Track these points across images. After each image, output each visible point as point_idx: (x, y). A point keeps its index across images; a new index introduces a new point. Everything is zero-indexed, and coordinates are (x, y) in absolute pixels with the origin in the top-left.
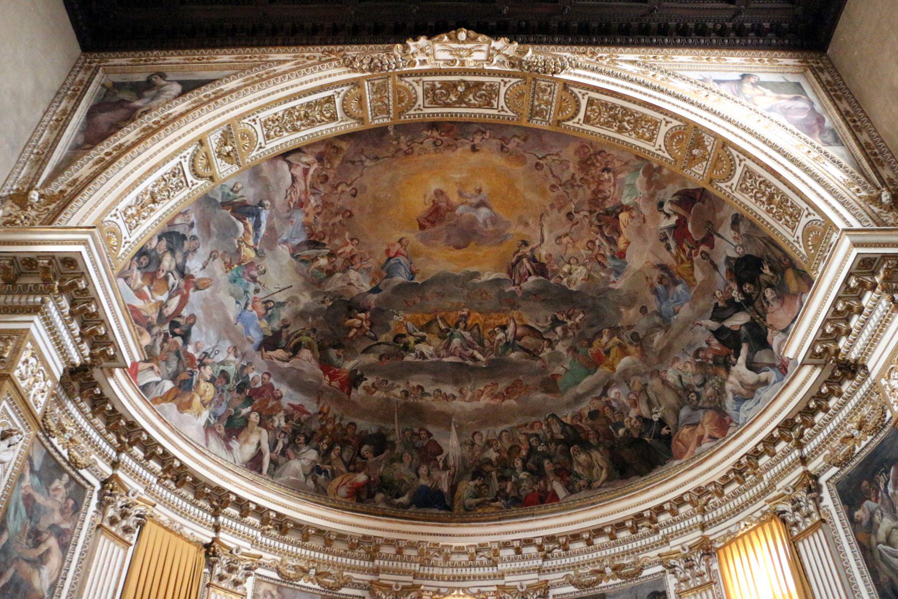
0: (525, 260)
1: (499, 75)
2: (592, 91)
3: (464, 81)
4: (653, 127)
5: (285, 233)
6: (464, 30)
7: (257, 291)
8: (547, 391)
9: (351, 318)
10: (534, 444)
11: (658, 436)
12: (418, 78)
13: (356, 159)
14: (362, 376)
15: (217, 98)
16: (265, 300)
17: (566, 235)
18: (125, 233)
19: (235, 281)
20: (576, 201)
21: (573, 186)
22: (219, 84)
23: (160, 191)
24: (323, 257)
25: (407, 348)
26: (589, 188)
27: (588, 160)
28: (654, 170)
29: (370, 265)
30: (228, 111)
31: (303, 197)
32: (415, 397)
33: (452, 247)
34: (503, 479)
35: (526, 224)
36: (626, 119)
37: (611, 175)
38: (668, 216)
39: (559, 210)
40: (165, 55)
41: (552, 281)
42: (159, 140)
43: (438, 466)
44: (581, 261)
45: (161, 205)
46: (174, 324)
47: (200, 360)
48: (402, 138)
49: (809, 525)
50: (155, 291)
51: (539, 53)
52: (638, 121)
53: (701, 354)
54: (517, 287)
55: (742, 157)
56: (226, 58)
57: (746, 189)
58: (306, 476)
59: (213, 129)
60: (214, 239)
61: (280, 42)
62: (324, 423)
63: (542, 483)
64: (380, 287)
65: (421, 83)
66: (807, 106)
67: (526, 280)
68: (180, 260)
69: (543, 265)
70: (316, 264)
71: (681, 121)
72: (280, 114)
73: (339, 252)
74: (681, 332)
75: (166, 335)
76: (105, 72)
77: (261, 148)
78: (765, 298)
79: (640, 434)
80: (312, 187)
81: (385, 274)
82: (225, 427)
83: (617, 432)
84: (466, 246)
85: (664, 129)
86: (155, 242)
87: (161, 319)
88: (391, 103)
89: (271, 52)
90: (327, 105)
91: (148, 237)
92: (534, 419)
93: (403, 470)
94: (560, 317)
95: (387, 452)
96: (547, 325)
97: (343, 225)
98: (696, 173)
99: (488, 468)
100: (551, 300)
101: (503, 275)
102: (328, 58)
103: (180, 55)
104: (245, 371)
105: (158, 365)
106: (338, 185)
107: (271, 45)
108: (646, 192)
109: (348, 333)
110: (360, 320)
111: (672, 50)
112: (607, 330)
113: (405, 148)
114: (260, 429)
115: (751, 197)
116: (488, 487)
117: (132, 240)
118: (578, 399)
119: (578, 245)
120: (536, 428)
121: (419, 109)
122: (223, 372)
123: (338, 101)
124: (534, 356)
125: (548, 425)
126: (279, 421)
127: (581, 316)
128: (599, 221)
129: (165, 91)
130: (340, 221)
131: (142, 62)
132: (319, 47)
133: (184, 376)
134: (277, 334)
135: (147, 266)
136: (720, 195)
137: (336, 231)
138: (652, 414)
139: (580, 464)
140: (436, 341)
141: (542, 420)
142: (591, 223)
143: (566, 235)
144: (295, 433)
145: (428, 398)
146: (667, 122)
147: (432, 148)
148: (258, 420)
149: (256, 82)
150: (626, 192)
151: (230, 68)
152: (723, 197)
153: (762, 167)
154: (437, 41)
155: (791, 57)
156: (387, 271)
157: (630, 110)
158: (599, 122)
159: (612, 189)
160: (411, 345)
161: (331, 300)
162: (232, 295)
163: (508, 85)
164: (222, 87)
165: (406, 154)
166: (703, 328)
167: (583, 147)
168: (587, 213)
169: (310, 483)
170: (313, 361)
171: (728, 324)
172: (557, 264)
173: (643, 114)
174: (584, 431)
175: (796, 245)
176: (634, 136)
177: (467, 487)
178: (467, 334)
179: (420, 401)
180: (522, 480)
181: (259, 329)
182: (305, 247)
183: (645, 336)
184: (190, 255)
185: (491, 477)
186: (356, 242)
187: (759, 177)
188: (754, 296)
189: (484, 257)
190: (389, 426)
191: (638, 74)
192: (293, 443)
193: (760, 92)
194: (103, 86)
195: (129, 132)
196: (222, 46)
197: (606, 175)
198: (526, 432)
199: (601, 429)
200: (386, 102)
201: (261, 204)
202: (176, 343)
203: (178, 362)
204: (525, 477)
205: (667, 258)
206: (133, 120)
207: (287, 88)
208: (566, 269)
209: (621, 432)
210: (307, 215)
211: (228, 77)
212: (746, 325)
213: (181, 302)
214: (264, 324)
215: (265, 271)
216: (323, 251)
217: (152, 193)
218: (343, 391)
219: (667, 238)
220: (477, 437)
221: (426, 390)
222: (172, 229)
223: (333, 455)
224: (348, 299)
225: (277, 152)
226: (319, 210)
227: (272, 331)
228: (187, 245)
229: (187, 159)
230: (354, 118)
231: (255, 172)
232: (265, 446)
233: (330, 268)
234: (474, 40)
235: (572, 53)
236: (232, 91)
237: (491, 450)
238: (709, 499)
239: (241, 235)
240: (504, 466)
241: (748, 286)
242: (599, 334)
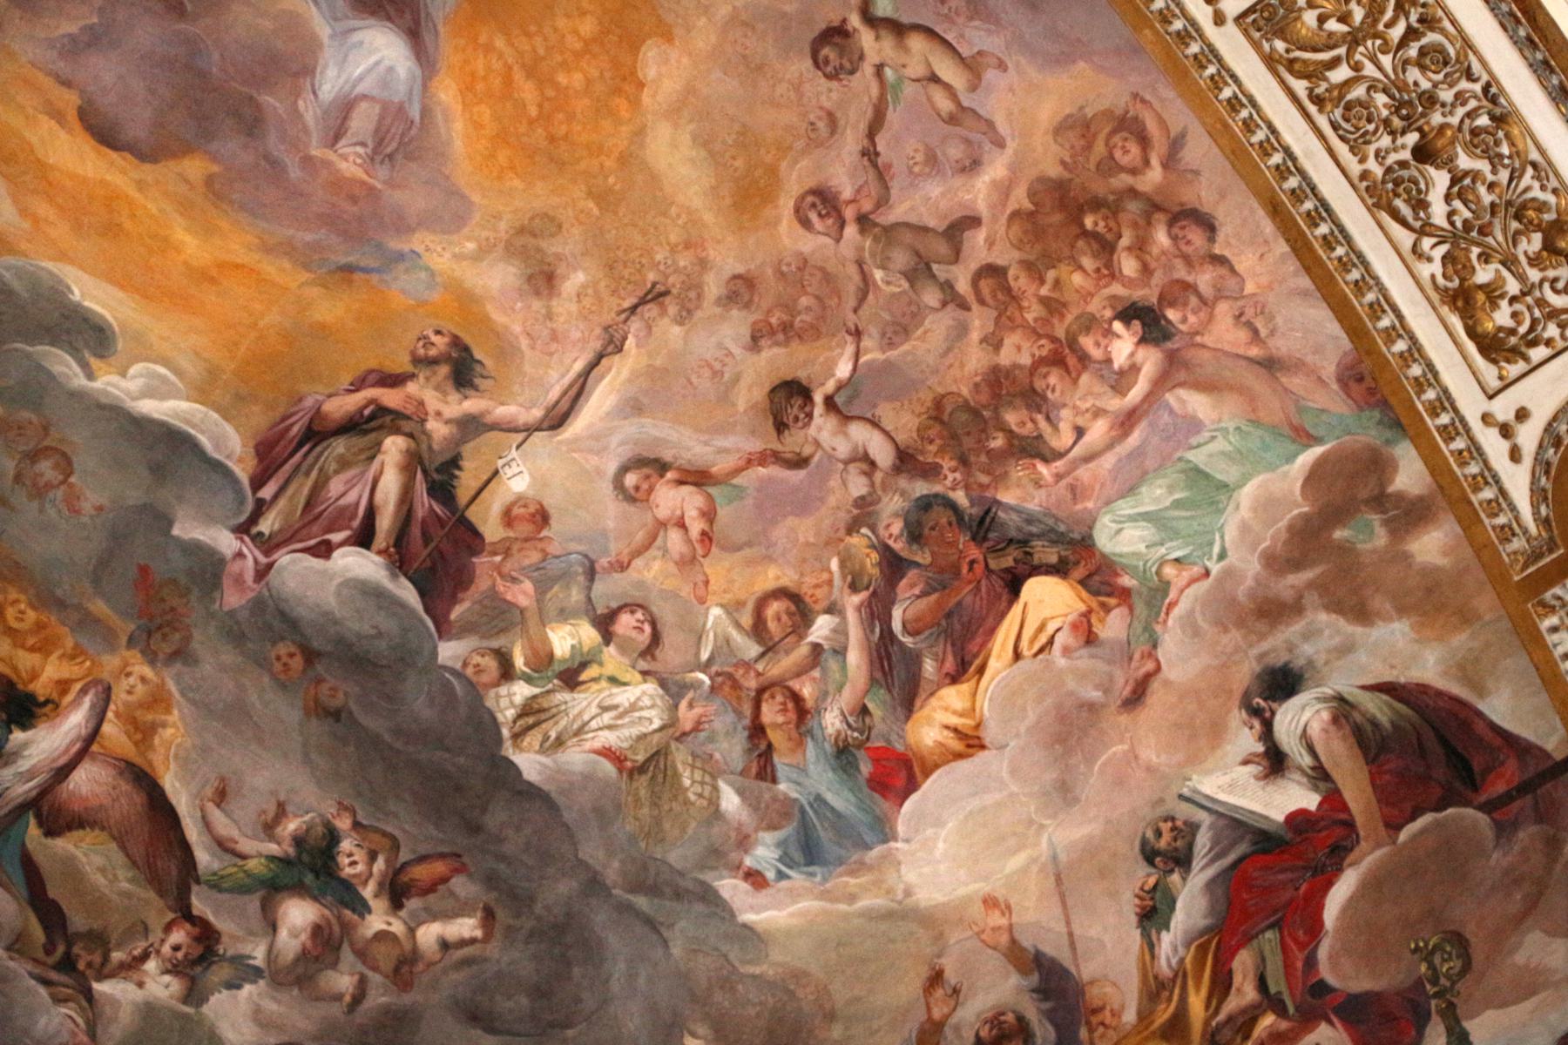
17: (698, 478)
20: (872, 355)
21: (920, 271)
26: (993, 342)
27: (1096, 204)
28: (1380, 501)
33: (70, 100)
35: (543, 280)
36: (1464, 162)
37: (1150, 361)
38: (1274, 762)
41: (449, 652)
44: (671, 655)
54: (252, 555)
67: (324, 550)
69: (468, 537)
84: (145, 154)
94: (351, 857)
96: (259, 850)
100: (376, 741)
108: (1252, 567)
119: (718, 568)
124: (67, 964)
127: (466, 927)
128: (915, 534)
142: (863, 514)
143: (698, 478)
150: (1156, 495)
159: (1098, 431)
168: (883, 453)
172: (542, 588)
189: (204, 277)
197: (1124, 346)
208: (563, 640)
219: (1181, 860)
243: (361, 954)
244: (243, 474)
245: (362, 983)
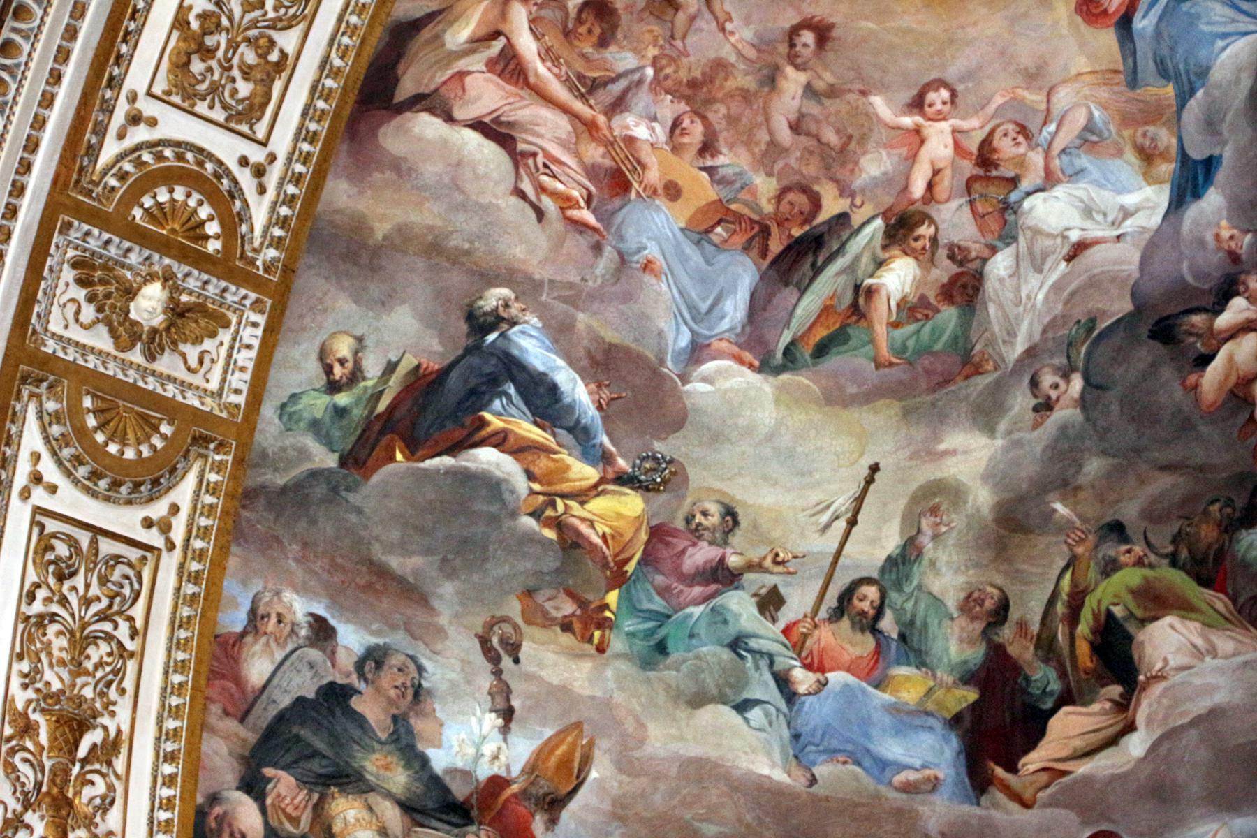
5: (664, 323)
7: (770, 602)
9: (1204, 360)
16: (831, 600)
19: (661, 648)
24: (880, 264)
29: (1079, 119)
31: (594, 153)
60: (446, 592)
64: (1196, 154)
68: (399, 779)
70: (881, 312)
77: (259, 172)
80: (588, 87)
81: (1170, 90)
97: (833, 92)
130: (809, 90)
137: (831, 137)
156: (1164, 72)
162: (698, 700)
170: (1225, 643)
182: (790, 294)
184: (418, 724)
201: (480, 323)
210: (673, 191)
215: (731, 515)
216: (857, 245)
222: (264, 715)
224: (1125, 306)
226: (696, 132)
227: (968, 678)
228: (369, 706)
233: (944, 270)
239: (521, 484)
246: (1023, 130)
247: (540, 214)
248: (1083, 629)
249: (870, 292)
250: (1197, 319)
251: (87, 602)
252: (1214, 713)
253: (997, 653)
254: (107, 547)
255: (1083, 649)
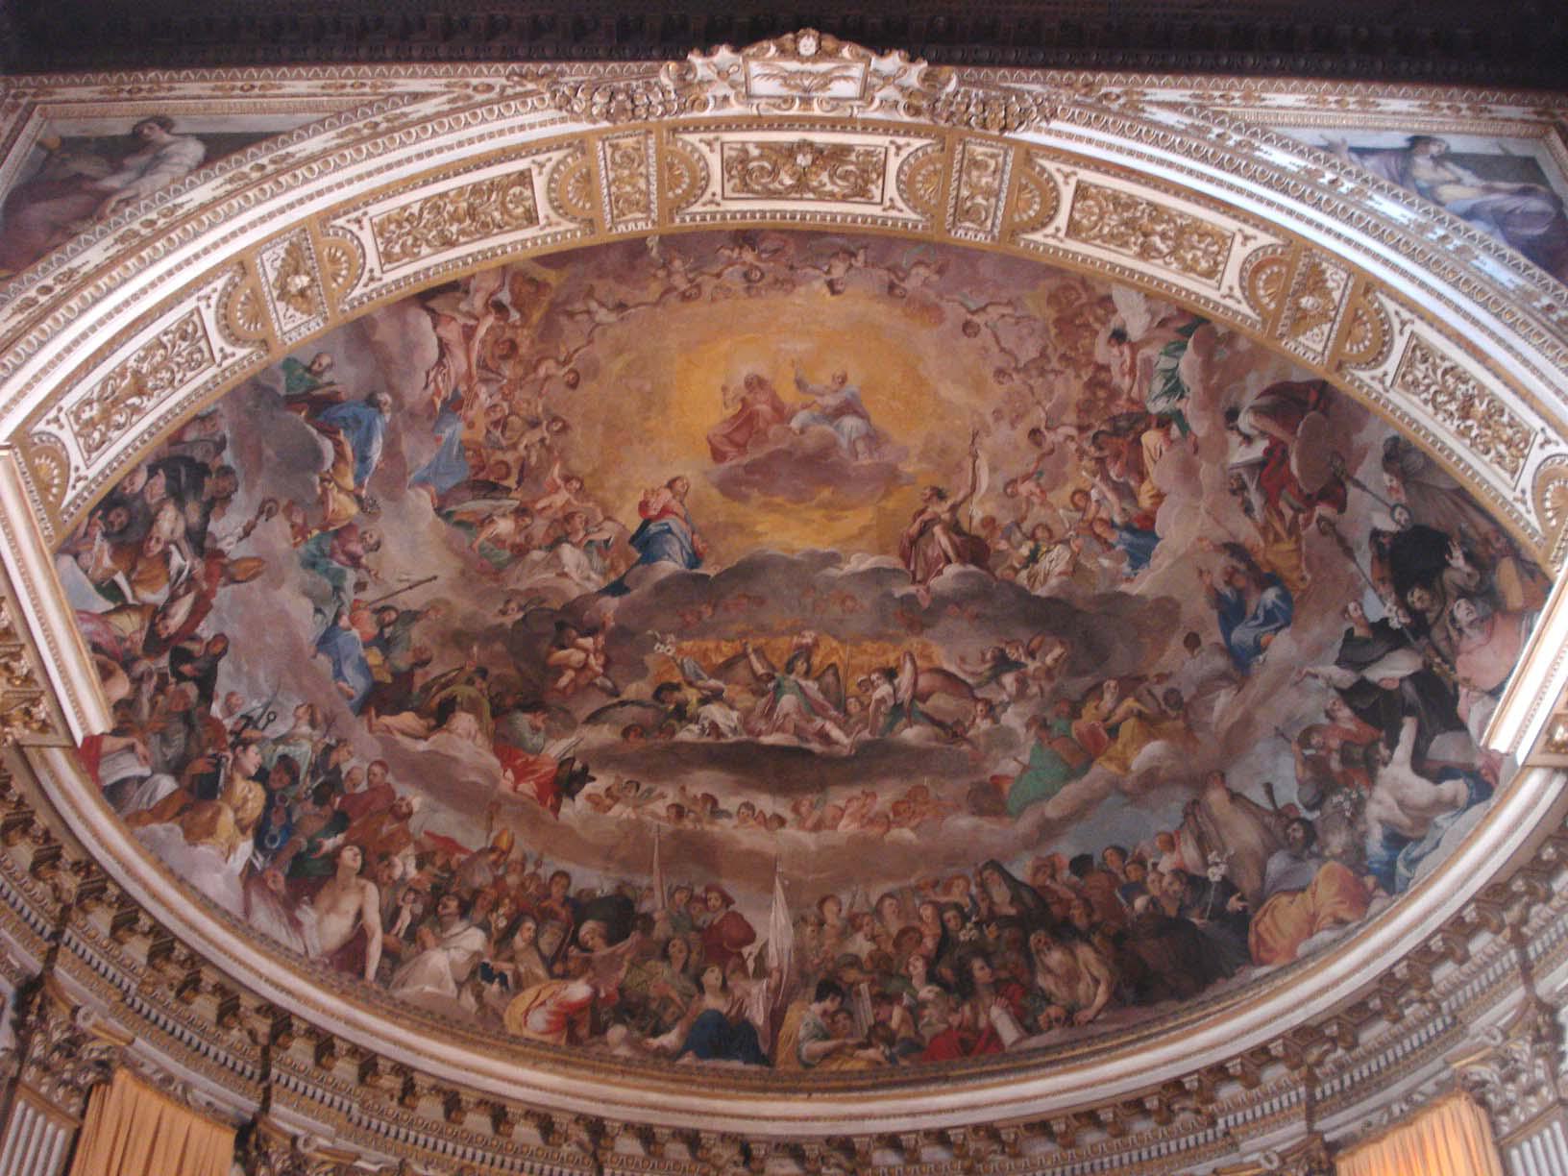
0: (937, 530)
1: (886, 132)
2: (1087, 167)
3: (811, 144)
4: (1215, 248)
6: (812, 32)
7: (360, 586)
8: (979, 811)
9: (563, 647)
10: (952, 925)
11: (1219, 914)
12: (711, 136)
13: (578, 306)
14: (585, 769)
15: (279, 172)
16: (379, 605)
17: (1027, 477)
18: (76, 458)
20: (1048, 406)
21: (1042, 373)
22: (284, 142)
23: (155, 370)
24: (504, 515)
25: (681, 714)
26: (1078, 376)
28: (1219, 341)
30: (301, 201)
32: (698, 820)
34: (884, 999)
36: (1159, 228)
38: (1248, 439)
39: (1013, 425)
40: (171, 80)
42: (153, 262)
43: (742, 966)
45: (154, 401)
46: (180, 656)
47: (236, 733)
48: (677, 264)
49: (1534, 1110)
50: (139, 582)
51: (974, 84)
52: (1185, 233)
53: (1316, 739)
54: (921, 589)
55: (1406, 315)
56: (302, 87)
57: (1415, 383)
58: (460, 985)
59: (269, 239)
61: (415, 53)
62: (500, 872)
63: (967, 1008)
64: (627, 583)
65: (717, 146)
66: (1550, 209)
67: (940, 573)
68: (195, 518)
69: (977, 541)
71: (1275, 235)
72: (415, 209)
73: (540, 505)
74: (1273, 689)
75: (163, 677)
76: (44, 114)
77: (372, 279)
78: (1453, 620)
79: (1179, 910)
80: (483, 365)
82: (288, 877)
83: (1131, 903)
85: (1239, 253)
86: (141, 479)
87: (155, 643)
88: (654, 188)
89: (397, 75)
90: (517, 190)
91: (127, 467)
92: (951, 871)
93: (664, 978)
94: (1013, 654)
95: (635, 937)
98: (1307, 348)
99: (851, 975)
101: (893, 561)
102: (519, 89)
103: (203, 79)
104: (334, 757)
105: (145, 743)
106: (539, 362)
107: (397, 60)
109: (556, 680)
110: (580, 652)
111: (1262, 82)
112: (1112, 683)
113: (683, 286)
114: (363, 882)
115: (1426, 402)
116: (851, 1015)
117: (92, 473)
118: (1049, 830)
119: (1052, 497)
120: (956, 890)
121: (711, 202)
122: (284, 758)
123: (540, 182)
125: (983, 886)
126: (405, 865)
127: (1058, 651)
128: (1100, 449)
129: (168, 157)
131: (125, 95)
132: (500, 66)
133: (200, 766)
134: (404, 678)
135: (122, 532)
136: (1359, 396)
138: (1206, 865)
139: (1049, 971)
140: (745, 700)
141: (970, 872)
142: (1081, 453)
143: (1027, 477)
144: (438, 892)
145: (724, 821)
146: (1246, 238)
147: (739, 285)
148: (358, 864)
149: (363, 140)
151: (311, 109)
152: (1367, 401)
153: (1448, 337)
154: (755, 57)
155: (1517, 103)
157: (1166, 209)
158: (1100, 236)
159: (1127, 380)
160: (691, 709)
161: (521, 608)
162: (307, 594)
163: (904, 154)
164: (291, 149)
165: (685, 297)
166: (1321, 683)
167: (1067, 288)
168: (1073, 432)
169: (469, 1001)
170: (480, 739)
171: (1374, 674)
172: (1008, 539)
173: (1195, 220)
174: (1060, 901)
175: (1519, 506)
176: (1174, 266)
177: (805, 1016)
178: (811, 686)
179: (708, 828)
180: (923, 1004)
181: (365, 669)
183: (1195, 697)
185: (858, 994)
186: (576, 485)
187: (1443, 358)
188: (1431, 616)
190: (643, 881)
191: (1184, 132)
192: (432, 914)
193: (1449, 176)
194: (41, 145)
195: (89, 244)
196: (292, 62)
198: (933, 898)
199: (1096, 897)
200: (643, 186)
201: (372, 401)
202: (183, 694)
203: (188, 736)
204: (931, 996)
205: (1246, 531)
206: (100, 219)
207: (429, 153)
209: (1140, 903)
210: (471, 425)
211: (305, 127)
212: (1411, 677)
213: (195, 603)
214: (374, 658)
215: (378, 545)
217: (137, 373)
218: (543, 803)
219: (1243, 487)
220: (830, 908)
221: (723, 805)
223: (519, 941)
225: (407, 291)
228: (209, 485)
229: (213, 302)
230: (573, 219)
231: (360, 332)
232: (373, 919)
233: (519, 539)
234: (832, 55)
235: (1044, 83)
236: (312, 158)
237: (860, 938)
238: (1327, 1053)
239: (328, 464)
240: (886, 970)
241: (1417, 593)
242: (1096, 691)
243: (1034, 678)
244: (901, 566)
245: (1041, 689)
246: (587, 522)
247: (427, 386)
248: (443, 694)
249: (492, 521)
250: (574, 633)
251: (179, 354)
252: (454, 760)
253: (409, 675)
254: (203, 344)
255: (437, 700)
